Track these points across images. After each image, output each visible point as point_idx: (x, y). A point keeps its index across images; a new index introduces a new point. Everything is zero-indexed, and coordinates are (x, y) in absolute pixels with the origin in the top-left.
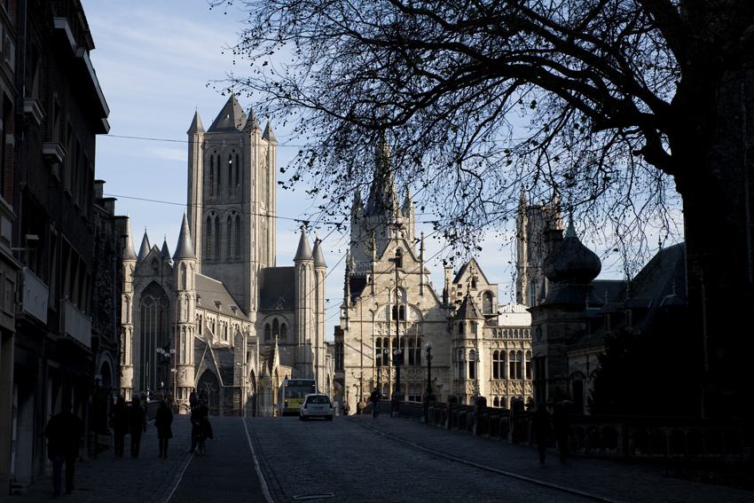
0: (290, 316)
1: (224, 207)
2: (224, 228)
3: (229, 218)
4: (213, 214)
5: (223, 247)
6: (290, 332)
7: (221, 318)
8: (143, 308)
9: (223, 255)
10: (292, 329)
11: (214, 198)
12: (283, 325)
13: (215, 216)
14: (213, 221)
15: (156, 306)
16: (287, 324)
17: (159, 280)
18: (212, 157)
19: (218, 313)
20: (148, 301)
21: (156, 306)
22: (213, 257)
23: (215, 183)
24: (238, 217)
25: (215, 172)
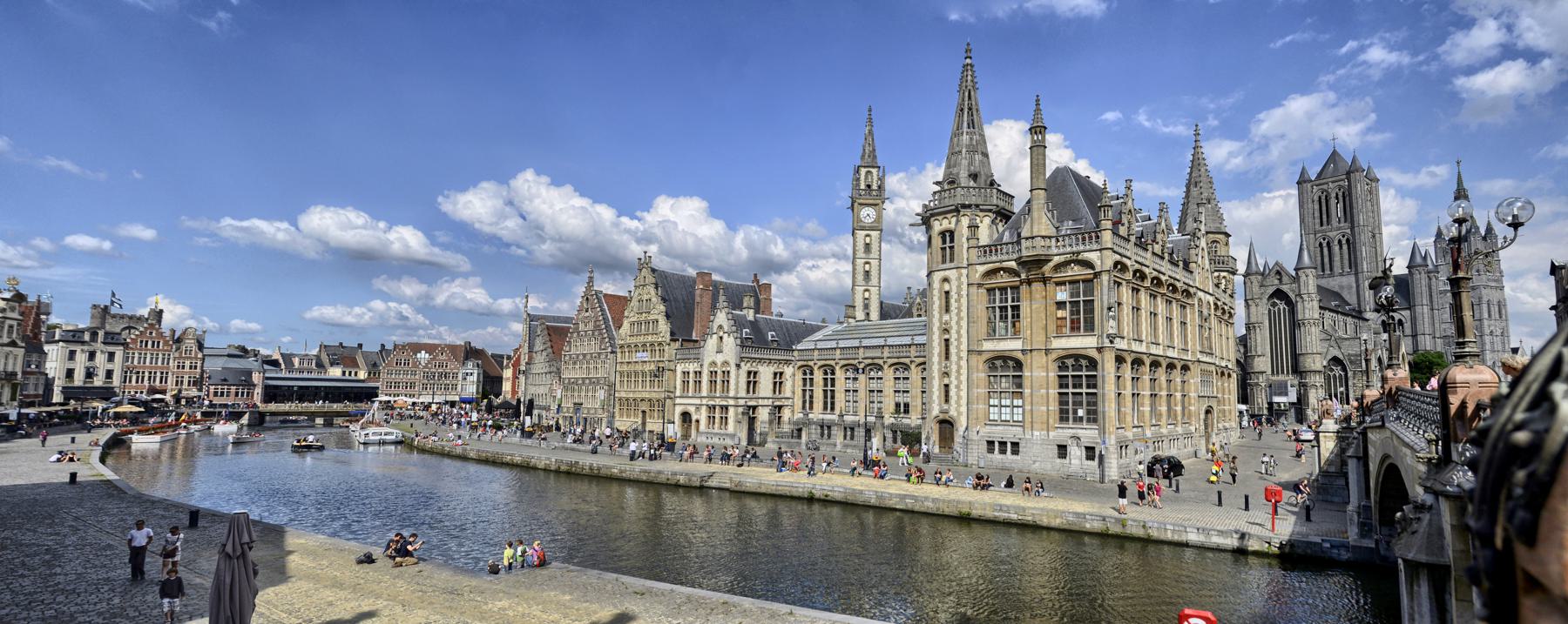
0: (1406, 313)
1: (1335, 233)
2: (1337, 248)
3: (1340, 241)
4: (1324, 239)
5: (1337, 263)
6: (1407, 325)
7: (1340, 316)
8: (1270, 310)
9: (1337, 270)
10: (1409, 323)
11: (1323, 228)
12: (1400, 321)
13: (1326, 240)
14: (1325, 245)
15: (1282, 308)
16: (1404, 320)
17: (1285, 288)
18: (1320, 198)
19: (1337, 312)
20: (1274, 305)
21: (1282, 308)
22: (1328, 272)
23: (1324, 216)
24: (1348, 240)
25: (1324, 208)
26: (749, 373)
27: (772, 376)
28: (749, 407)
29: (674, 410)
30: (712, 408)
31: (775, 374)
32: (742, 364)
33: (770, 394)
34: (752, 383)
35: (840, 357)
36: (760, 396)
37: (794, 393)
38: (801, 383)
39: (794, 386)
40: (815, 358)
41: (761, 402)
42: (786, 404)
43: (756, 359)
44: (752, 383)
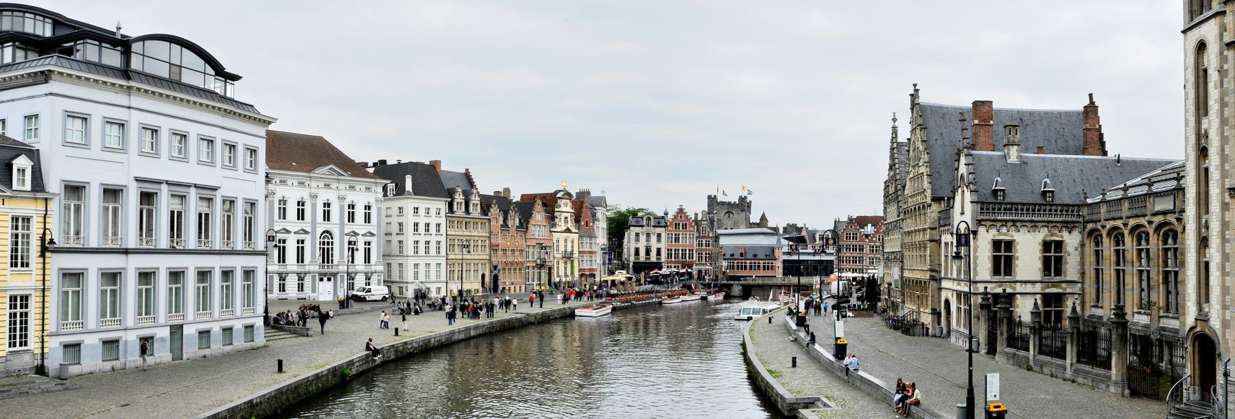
26: (997, 244)
27: (1040, 247)
28: (996, 297)
29: (940, 296)
30: (959, 294)
31: (1046, 246)
32: (982, 230)
33: (1037, 275)
34: (1003, 259)
35: (1129, 214)
36: (1018, 278)
37: (1083, 274)
38: (1093, 259)
39: (1082, 263)
40: (1102, 217)
41: (1019, 288)
42: (1068, 290)
43: (1006, 221)
44: (1003, 259)
